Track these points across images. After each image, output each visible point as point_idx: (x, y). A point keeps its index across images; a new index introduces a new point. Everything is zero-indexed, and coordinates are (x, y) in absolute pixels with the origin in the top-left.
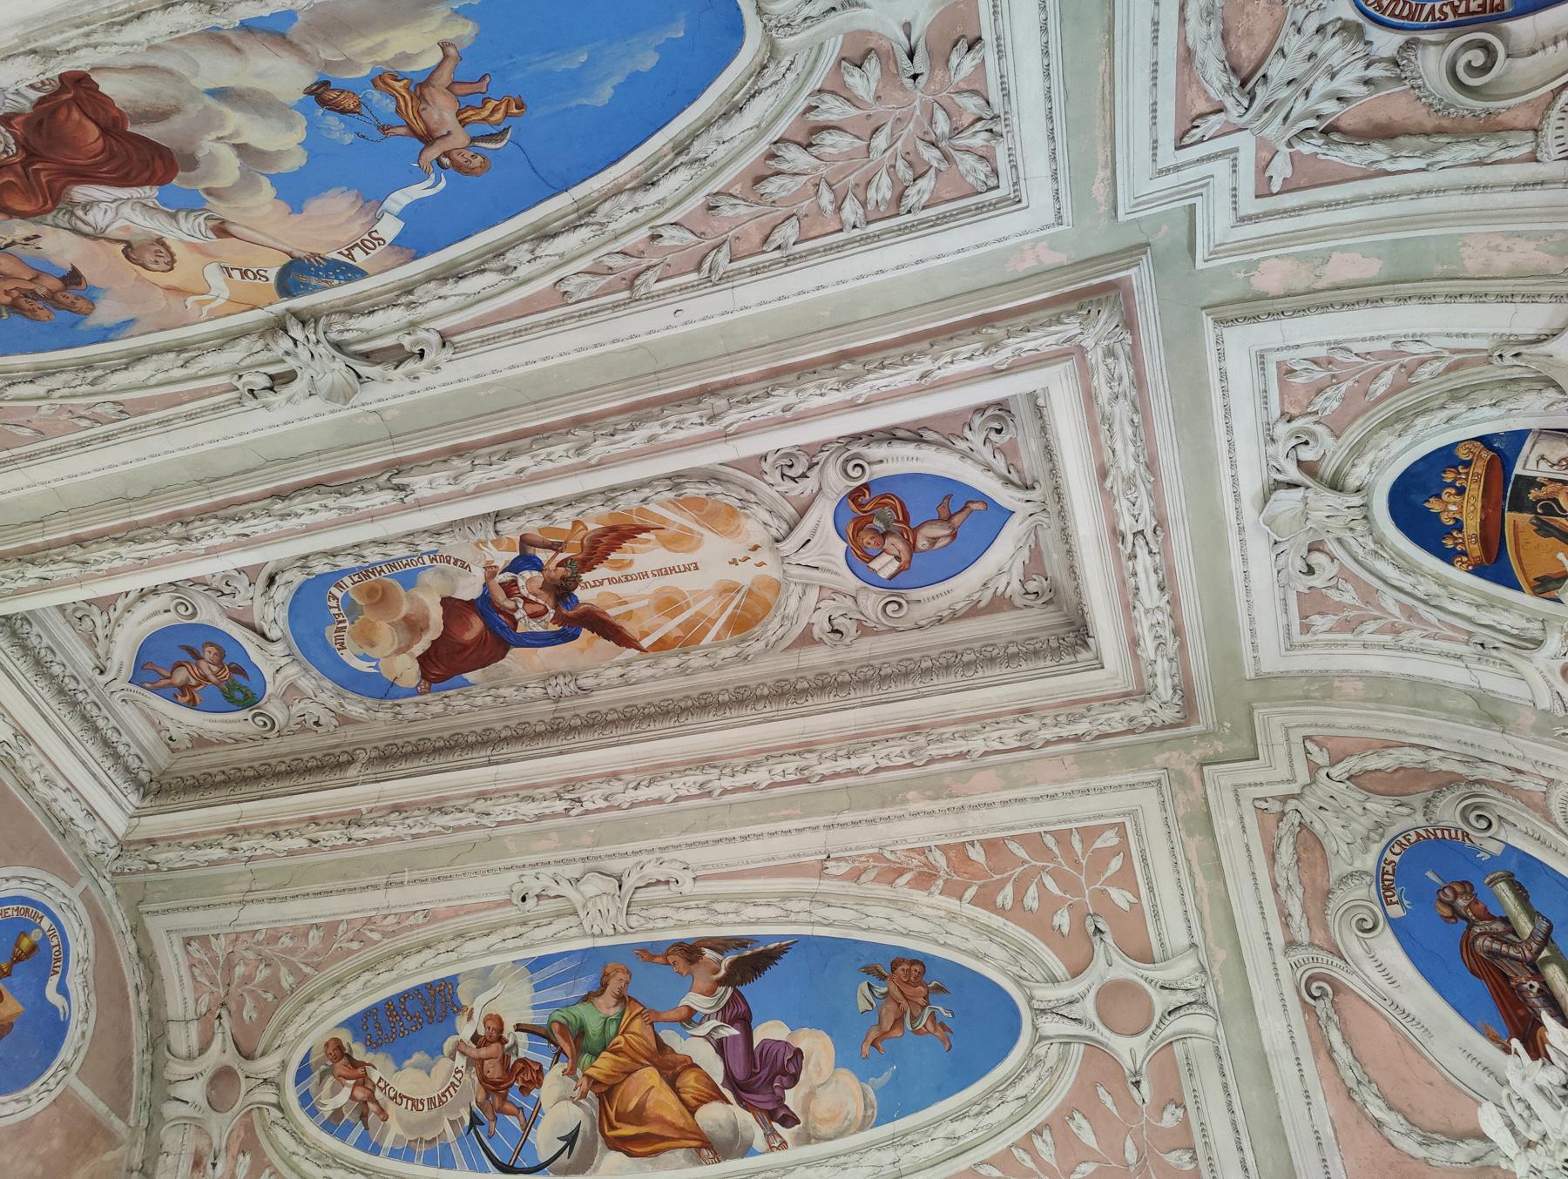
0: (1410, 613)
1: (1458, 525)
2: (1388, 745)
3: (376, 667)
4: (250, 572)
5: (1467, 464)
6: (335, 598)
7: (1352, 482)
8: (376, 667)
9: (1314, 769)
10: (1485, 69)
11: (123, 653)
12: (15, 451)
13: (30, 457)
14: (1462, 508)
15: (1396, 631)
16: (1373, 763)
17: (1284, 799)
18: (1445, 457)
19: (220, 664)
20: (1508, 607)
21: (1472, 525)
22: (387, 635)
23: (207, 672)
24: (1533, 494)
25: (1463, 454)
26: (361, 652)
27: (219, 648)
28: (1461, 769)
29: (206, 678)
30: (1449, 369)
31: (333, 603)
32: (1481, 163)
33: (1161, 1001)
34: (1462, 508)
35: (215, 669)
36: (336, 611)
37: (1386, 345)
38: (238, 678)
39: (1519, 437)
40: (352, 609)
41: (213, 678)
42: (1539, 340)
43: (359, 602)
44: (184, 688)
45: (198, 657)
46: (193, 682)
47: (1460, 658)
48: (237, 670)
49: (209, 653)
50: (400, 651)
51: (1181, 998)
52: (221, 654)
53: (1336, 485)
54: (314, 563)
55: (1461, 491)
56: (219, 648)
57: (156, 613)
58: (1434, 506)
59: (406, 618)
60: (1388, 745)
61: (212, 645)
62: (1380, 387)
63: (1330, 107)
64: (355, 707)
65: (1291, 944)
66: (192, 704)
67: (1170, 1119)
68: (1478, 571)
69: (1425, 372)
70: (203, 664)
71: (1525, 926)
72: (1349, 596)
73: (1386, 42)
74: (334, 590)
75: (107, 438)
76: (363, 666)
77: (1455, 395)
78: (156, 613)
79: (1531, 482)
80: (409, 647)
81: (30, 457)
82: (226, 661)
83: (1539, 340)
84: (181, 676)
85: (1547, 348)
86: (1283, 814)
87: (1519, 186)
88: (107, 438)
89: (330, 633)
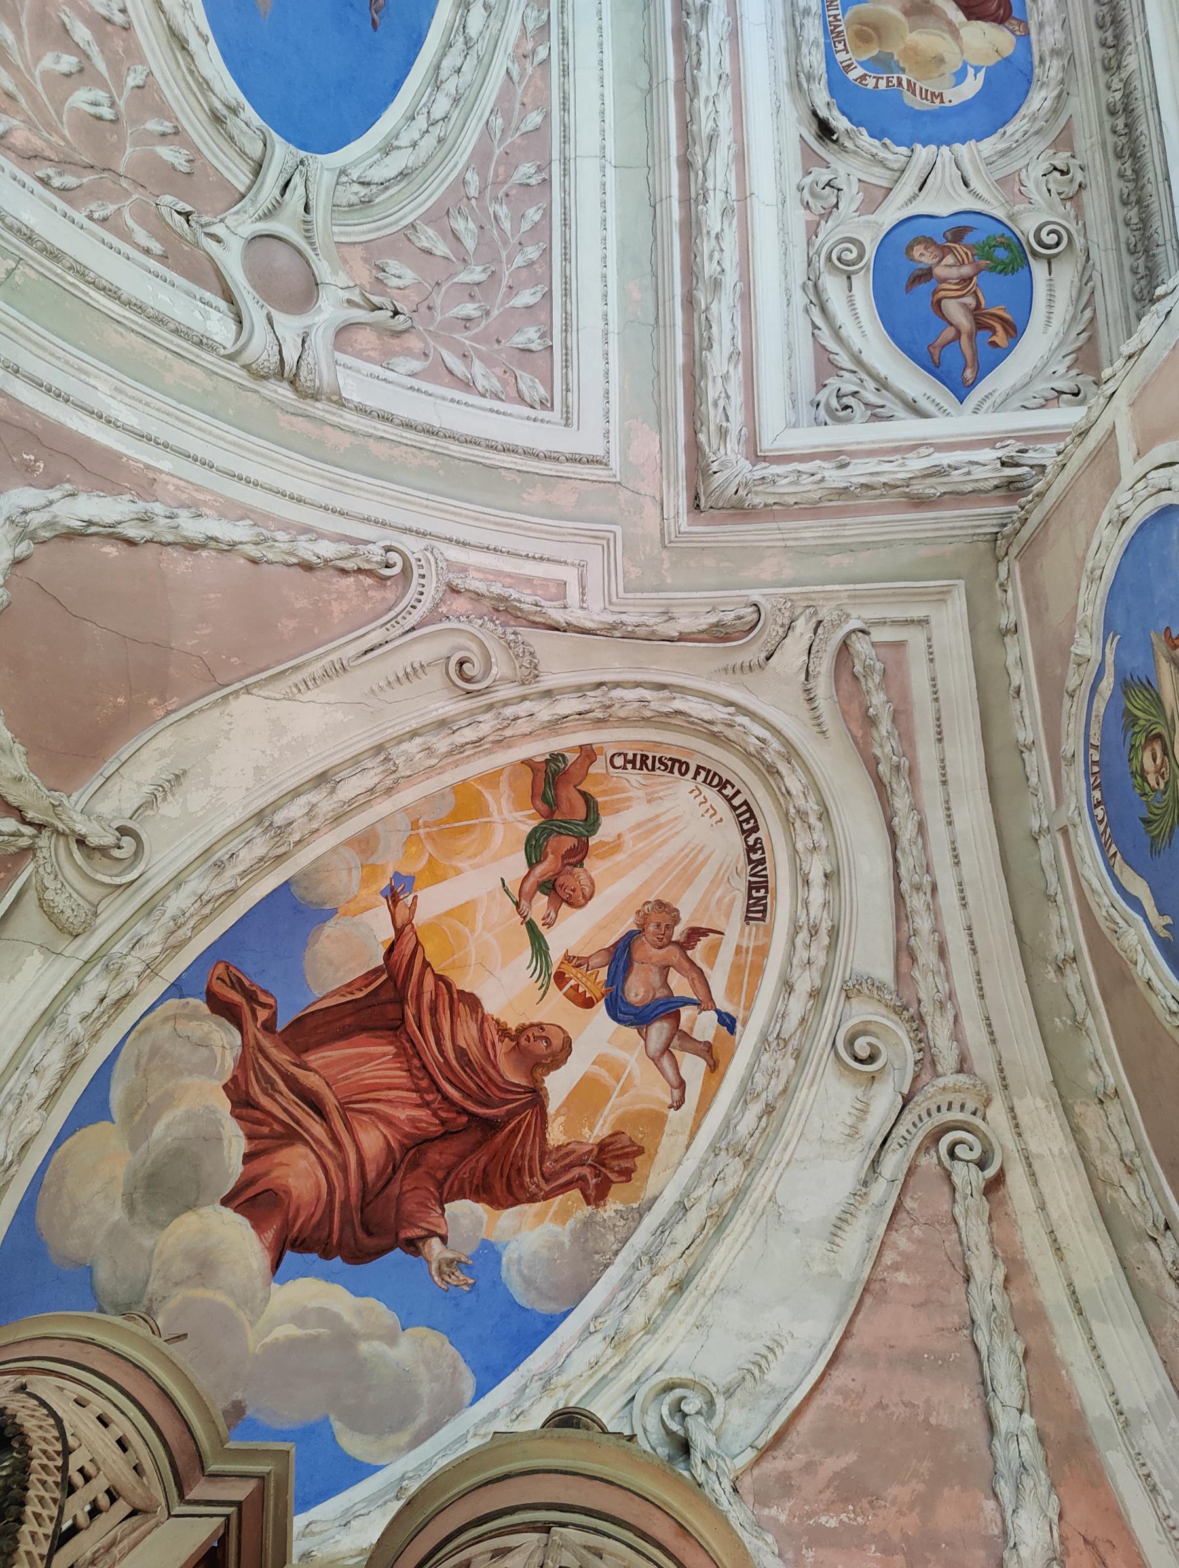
3: (977, 70)
4: (810, 159)
6: (863, 77)
8: (977, 70)
11: (912, 381)
12: (555, 154)
13: (565, 139)
19: (944, 251)
22: (928, 40)
23: (954, 272)
26: (949, 79)
27: (917, 241)
29: (965, 281)
31: (871, 83)
35: (950, 259)
36: (882, 84)
38: (969, 238)
40: (883, 64)
41: (966, 270)
43: (875, 53)
44: (980, 320)
45: (926, 275)
46: (970, 301)
48: (958, 234)
49: (924, 257)
50: (954, 32)
52: (928, 242)
54: (806, 63)
56: (917, 241)
57: (851, 302)
59: (907, 13)
61: (910, 248)
64: (1039, 100)
66: (1015, 331)
70: (939, 271)
74: (853, 75)
75: (564, 42)
76: (972, 86)
78: (851, 302)
80: (950, 23)
81: (565, 139)
82: (941, 241)
84: (956, 311)
88: (564, 42)
89: (915, 102)
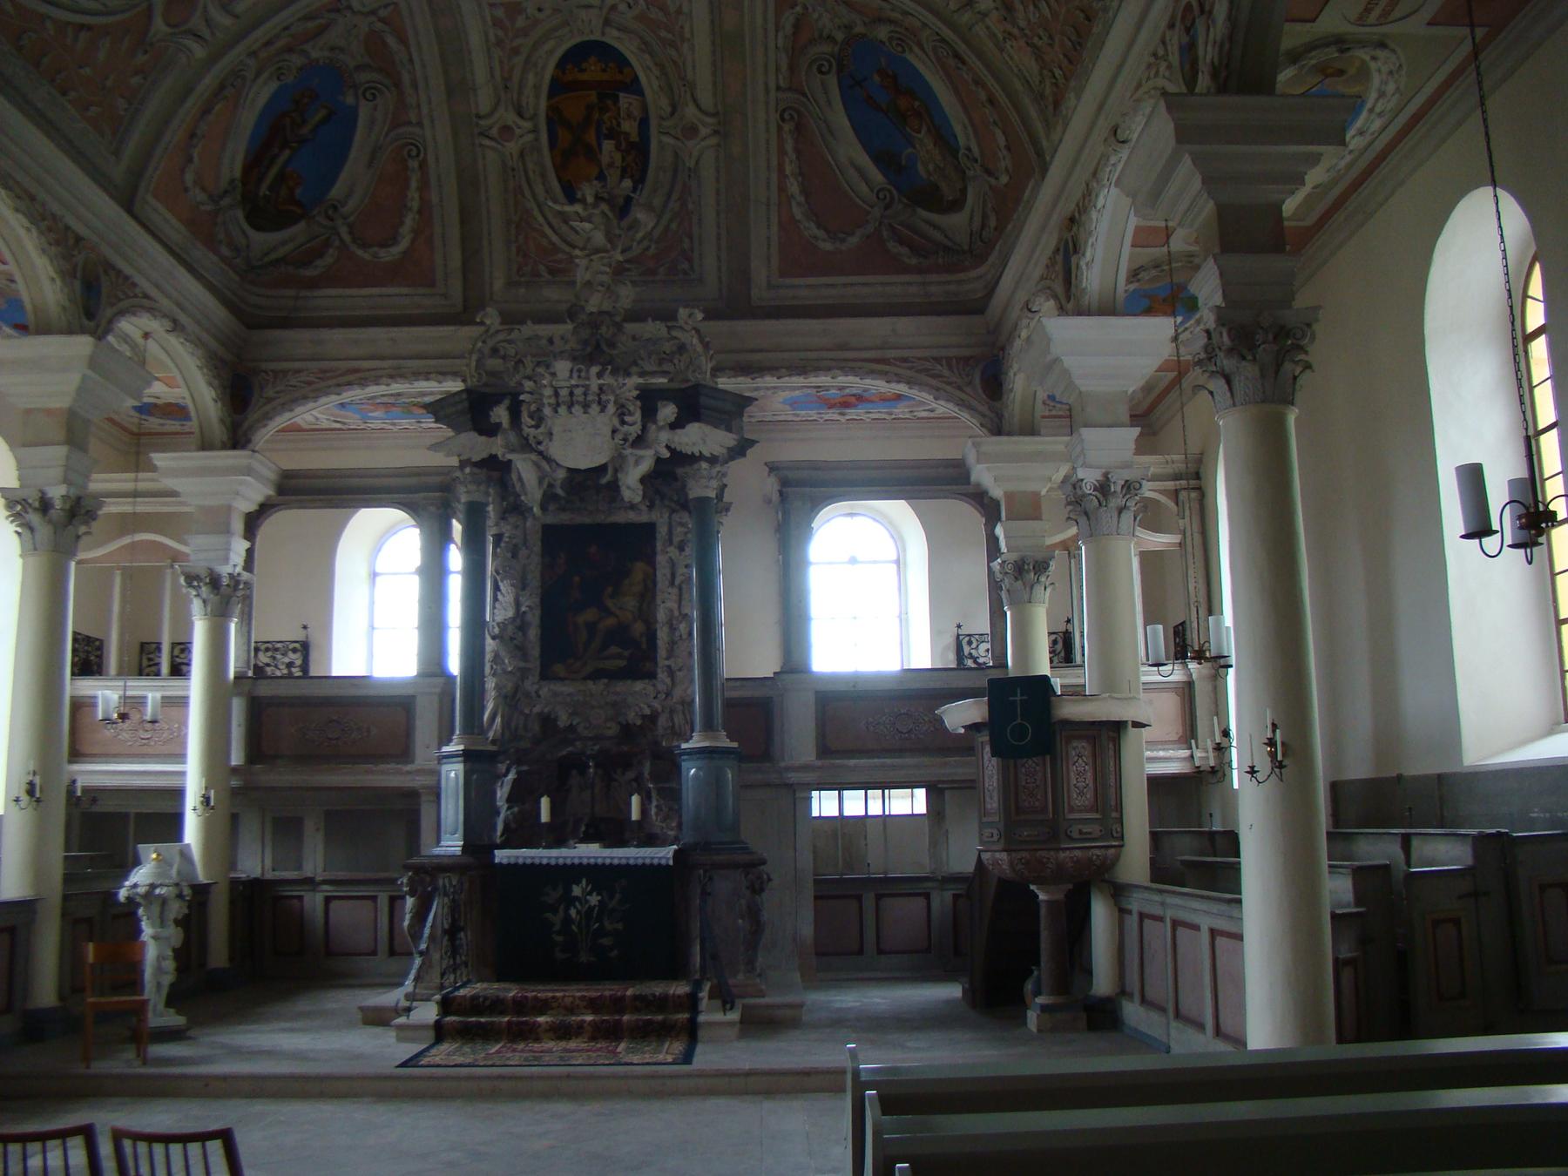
0: (516, 51)
1: (582, 71)
2: (403, 41)
5: (621, 72)
7: (608, 30)
9: (373, 12)
10: (821, 72)
14: (593, 70)
15: (499, 43)
16: (391, 41)
17: (349, 7)
18: (622, 63)
20: (537, 97)
21: (585, 77)
24: (609, 102)
25: (626, 71)
28: (406, 78)
30: (675, 62)
32: (778, 69)
33: (196, 22)
34: (593, 70)
37: (687, 35)
39: (640, 92)
42: (695, 101)
47: (492, 76)
51: (206, 33)
53: (607, 22)
55: (604, 71)
58: (592, 59)
60: (403, 41)
62: (663, 34)
63: (815, 16)
65: (253, 54)
67: (135, 80)
68: (554, 80)
69: (673, 53)
71: (305, 131)
72: (520, 22)
73: (840, 36)
77: (661, 66)
79: (616, 100)
83: (695, 101)
85: (691, 104)
86: (338, 11)
87: (766, 84)
